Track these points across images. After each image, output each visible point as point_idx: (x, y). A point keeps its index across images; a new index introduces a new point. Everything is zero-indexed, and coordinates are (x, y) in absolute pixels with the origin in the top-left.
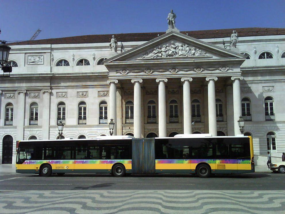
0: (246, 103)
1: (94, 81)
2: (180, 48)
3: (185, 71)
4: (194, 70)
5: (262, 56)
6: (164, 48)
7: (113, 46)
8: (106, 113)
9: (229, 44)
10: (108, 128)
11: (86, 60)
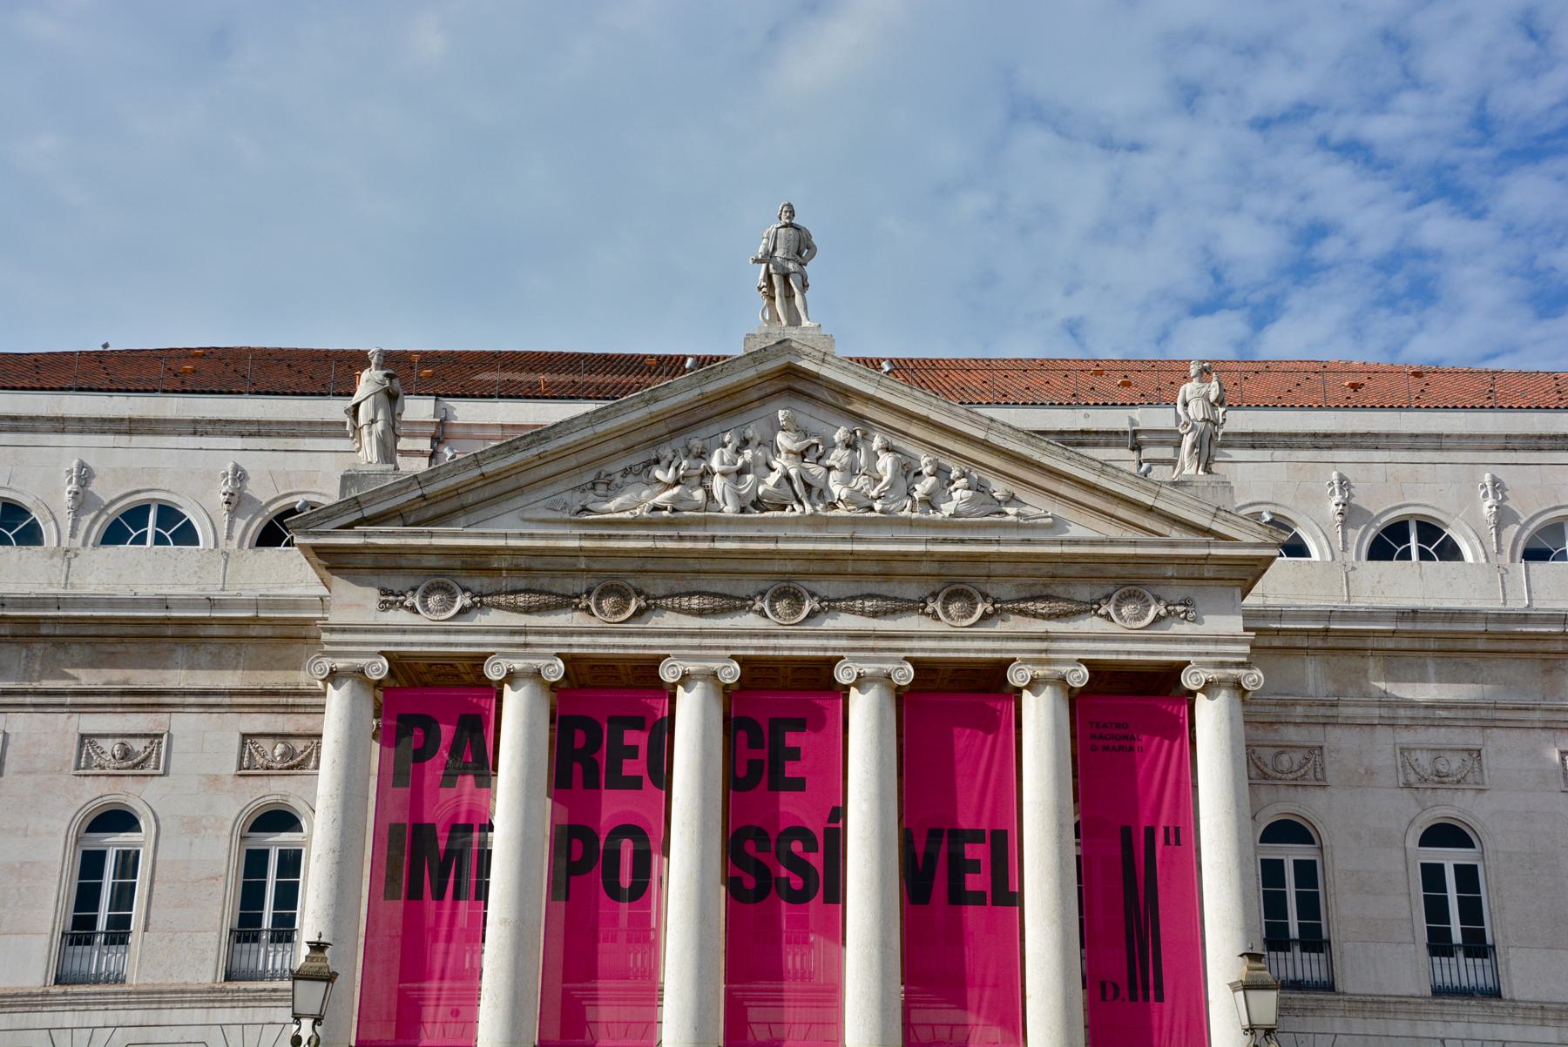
0: (1290, 854)
1: (218, 664)
2: (839, 456)
3: (863, 613)
4: (929, 610)
5: (1388, 544)
6: (727, 453)
7: (373, 421)
8: (288, 896)
9: (1167, 453)
10: (285, 1015)
11: (169, 514)
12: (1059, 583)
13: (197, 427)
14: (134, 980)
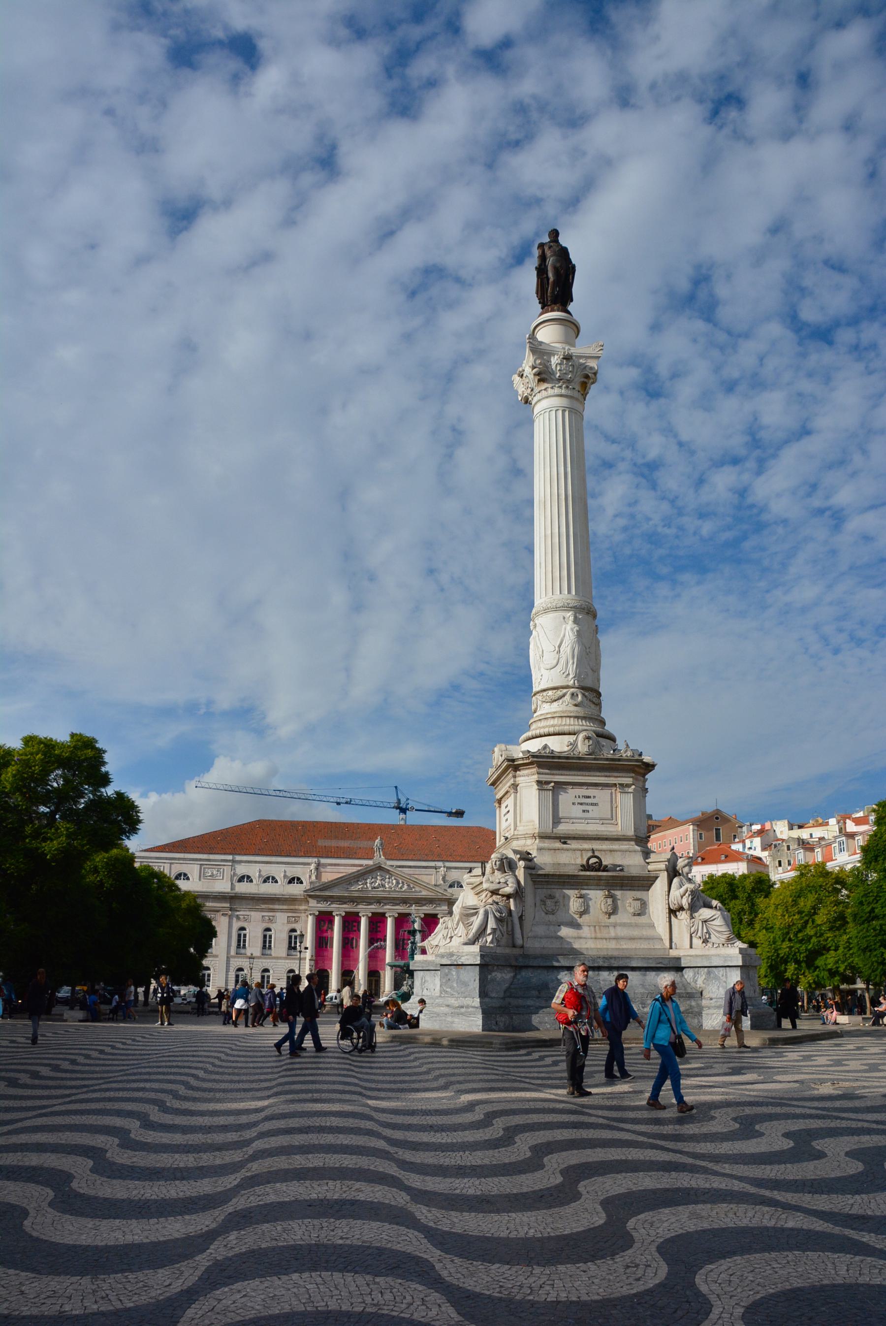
11: (273, 878)
12: (420, 901)
13: (278, 863)
14: (273, 955)
